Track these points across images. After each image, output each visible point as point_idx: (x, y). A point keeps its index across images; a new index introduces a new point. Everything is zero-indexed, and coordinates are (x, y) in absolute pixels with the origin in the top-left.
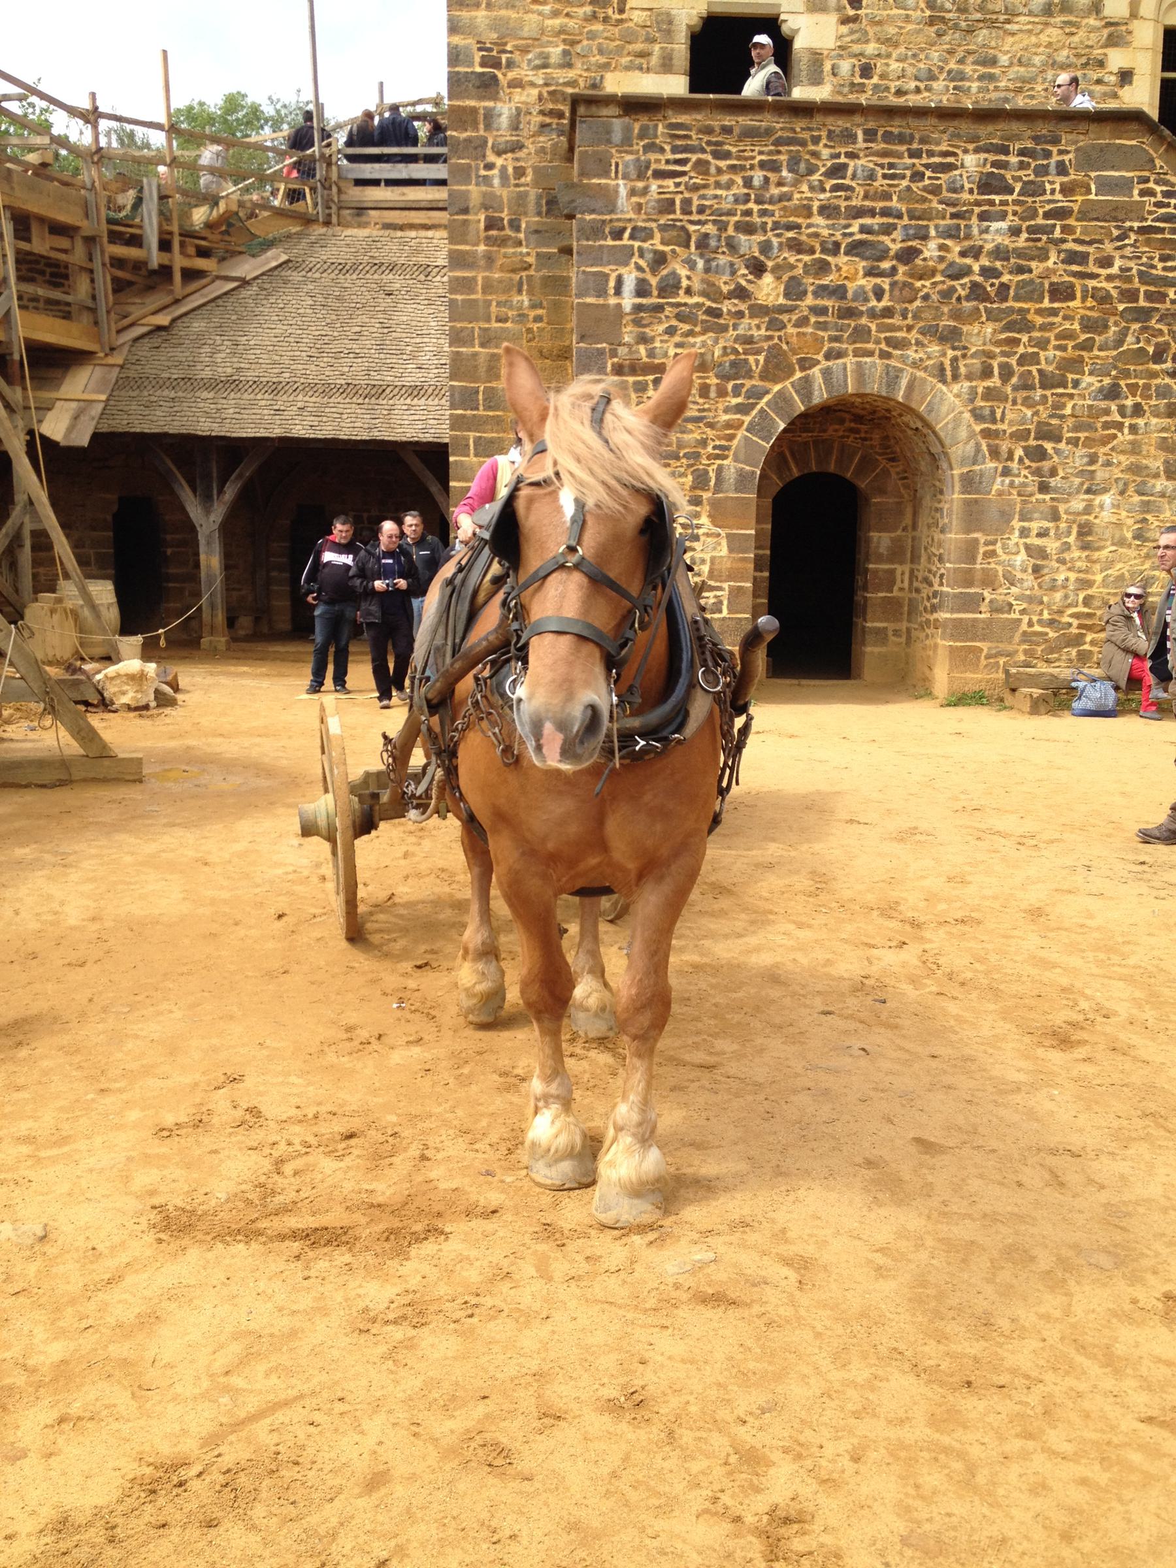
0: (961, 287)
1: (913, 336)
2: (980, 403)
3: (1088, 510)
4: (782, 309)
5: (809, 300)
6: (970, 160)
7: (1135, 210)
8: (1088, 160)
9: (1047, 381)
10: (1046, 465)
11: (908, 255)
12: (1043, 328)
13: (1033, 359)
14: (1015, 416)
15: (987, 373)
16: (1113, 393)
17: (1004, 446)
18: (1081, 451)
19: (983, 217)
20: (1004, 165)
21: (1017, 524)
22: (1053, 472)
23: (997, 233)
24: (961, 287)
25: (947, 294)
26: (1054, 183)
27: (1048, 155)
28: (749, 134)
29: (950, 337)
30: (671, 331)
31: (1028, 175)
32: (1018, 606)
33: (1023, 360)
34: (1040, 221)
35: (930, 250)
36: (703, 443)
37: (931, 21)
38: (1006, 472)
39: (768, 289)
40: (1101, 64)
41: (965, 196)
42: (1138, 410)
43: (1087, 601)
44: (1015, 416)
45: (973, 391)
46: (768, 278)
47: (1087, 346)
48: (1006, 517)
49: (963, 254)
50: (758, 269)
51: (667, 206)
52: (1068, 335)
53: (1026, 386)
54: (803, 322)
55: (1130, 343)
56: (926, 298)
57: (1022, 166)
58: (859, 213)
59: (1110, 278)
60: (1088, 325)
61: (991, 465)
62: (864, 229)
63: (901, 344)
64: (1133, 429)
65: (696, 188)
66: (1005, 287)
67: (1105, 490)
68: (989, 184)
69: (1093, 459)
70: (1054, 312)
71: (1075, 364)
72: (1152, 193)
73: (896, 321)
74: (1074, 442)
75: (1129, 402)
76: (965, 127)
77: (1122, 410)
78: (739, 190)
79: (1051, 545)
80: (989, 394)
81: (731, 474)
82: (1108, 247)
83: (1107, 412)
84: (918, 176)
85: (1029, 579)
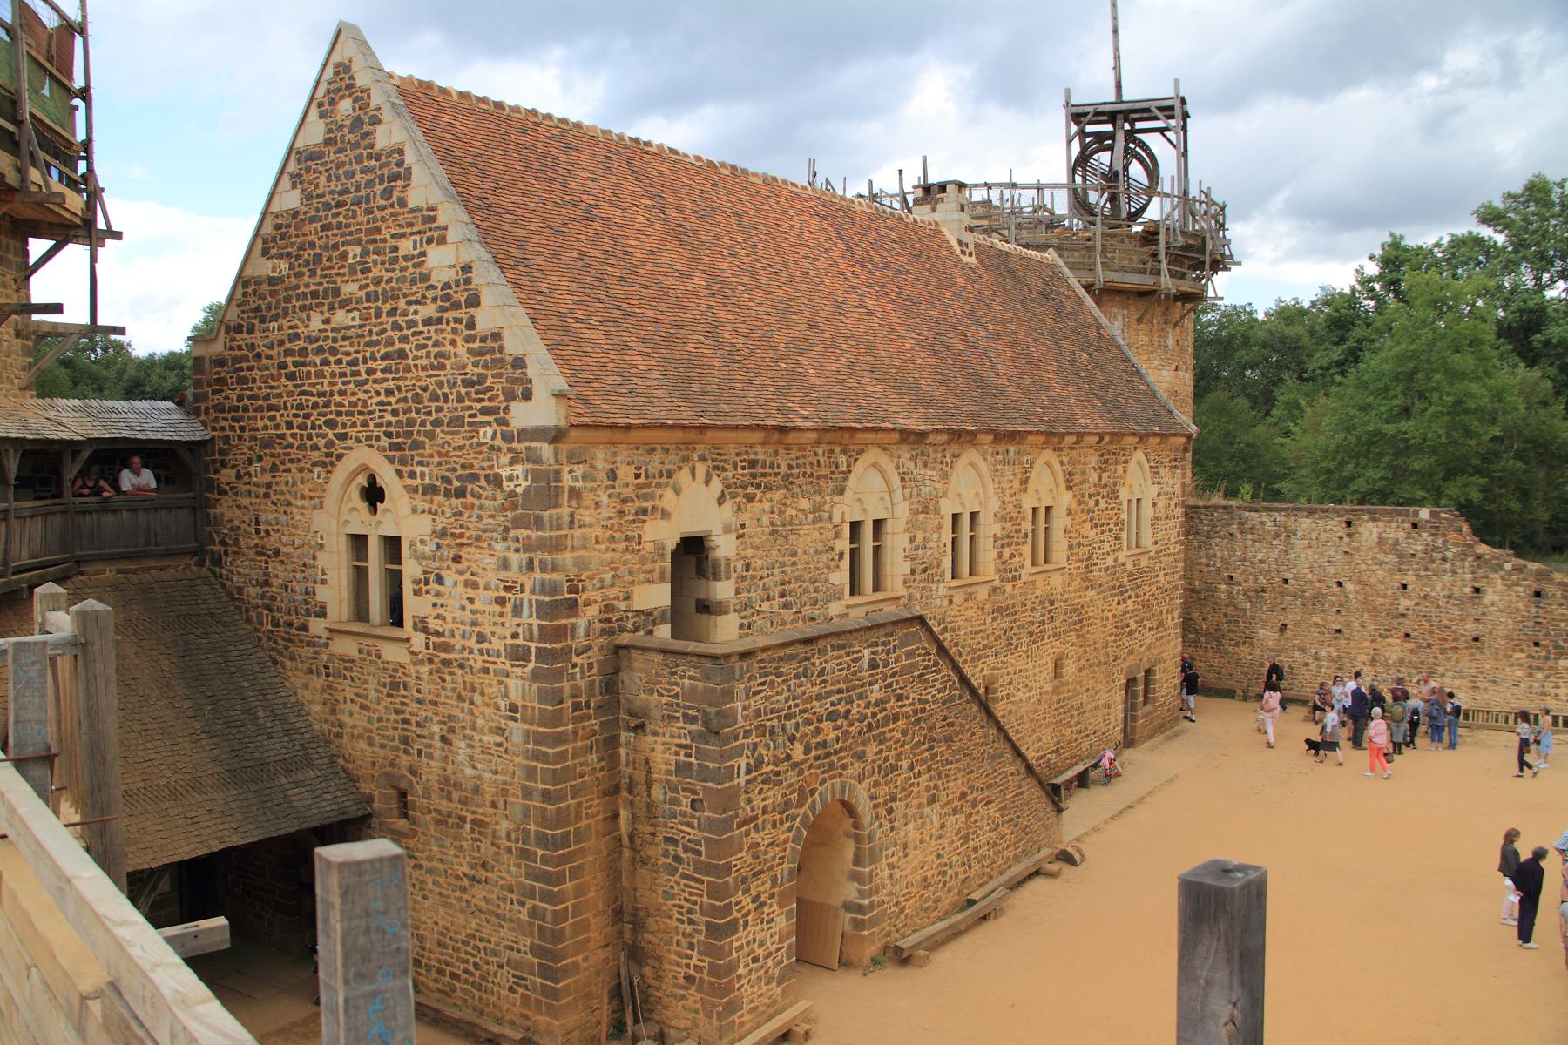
4: (803, 762)
5: (813, 753)
23: (876, 693)
28: (792, 657)
29: (860, 756)
30: (760, 792)
31: (884, 656)
36: (774, 858)
37: (772, 533)
39: (798, 752)
40: (832, 549)
46: (797, 744)
50: (792, 739)
51: (758, 714)
54: (810, 767)
58: (828, 694)
62: (833, 704)
65: (767, 698)
68: (873, 665)
71: (899, 757)
78: (786, 694)
81: (786, 873)
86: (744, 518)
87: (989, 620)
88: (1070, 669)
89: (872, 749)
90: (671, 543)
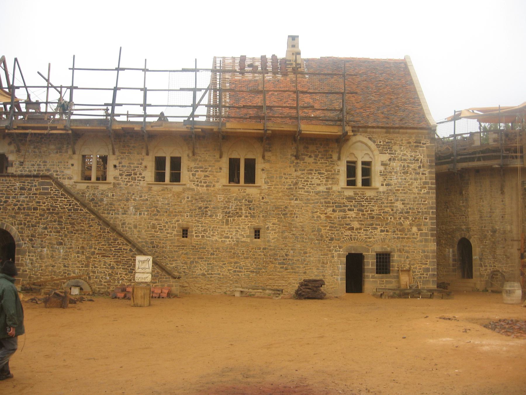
0: (16, 208)
1: (7, 217)
2: (20, 230)
3: (41, 251)
6: (18, 184)
7: (49, 193)
8: (41, 184)
9: (33, 226)
10: (33, 242)
11: (6, 202)
12: (32, 216)
13: (30, 222)
14: (27, 232)
15: (21, 224)
16: (46, 228)
17: (25, 238)
18: (40, 240)
19: (21, 195)
20: (25, 185)
21: (27, 254)
22: (34, 244)
23: (22, 198)
24: (16, 208)
25: (13, 209)
26: (34, 188)
27: (33, 183)
29: (14, 217)
31: (29, 187)
32: (28, 271)
33: (28, 222)
34: (31, 195)
35: (10, 201)
38: (25, 243)
41: (17, 191)
42: (51, 232)
43: (41, 270)
44: (27, 232)
45: (18, 228)
47: (41, 219)
48: (25, 253)
49: (17, 201)
52: (37, 217)
53: (29, 227)
55: (49, 219)
56: (9, 210)
57: (28, 185)
59: (45, 206)
60: (41, 215)
61: (22, 242)
63: (5, 218)
64: (50, 235)
66: (24, 208)
67: (45, 247)
68: (22, 189)
69: (42, 241)
70: (34, 213)
71: (39, 223)
72: (52, 190)
73: (4, 214)
74: (38, 238)
75: (49, 230)
76: (17, 178)
77: (48, 232)
79: (34, 259)
80: (22, 228)
82: (44, 200)
83: (45, 232)
84: (8, 187)
85: (30, 265)
88: (271, 236)
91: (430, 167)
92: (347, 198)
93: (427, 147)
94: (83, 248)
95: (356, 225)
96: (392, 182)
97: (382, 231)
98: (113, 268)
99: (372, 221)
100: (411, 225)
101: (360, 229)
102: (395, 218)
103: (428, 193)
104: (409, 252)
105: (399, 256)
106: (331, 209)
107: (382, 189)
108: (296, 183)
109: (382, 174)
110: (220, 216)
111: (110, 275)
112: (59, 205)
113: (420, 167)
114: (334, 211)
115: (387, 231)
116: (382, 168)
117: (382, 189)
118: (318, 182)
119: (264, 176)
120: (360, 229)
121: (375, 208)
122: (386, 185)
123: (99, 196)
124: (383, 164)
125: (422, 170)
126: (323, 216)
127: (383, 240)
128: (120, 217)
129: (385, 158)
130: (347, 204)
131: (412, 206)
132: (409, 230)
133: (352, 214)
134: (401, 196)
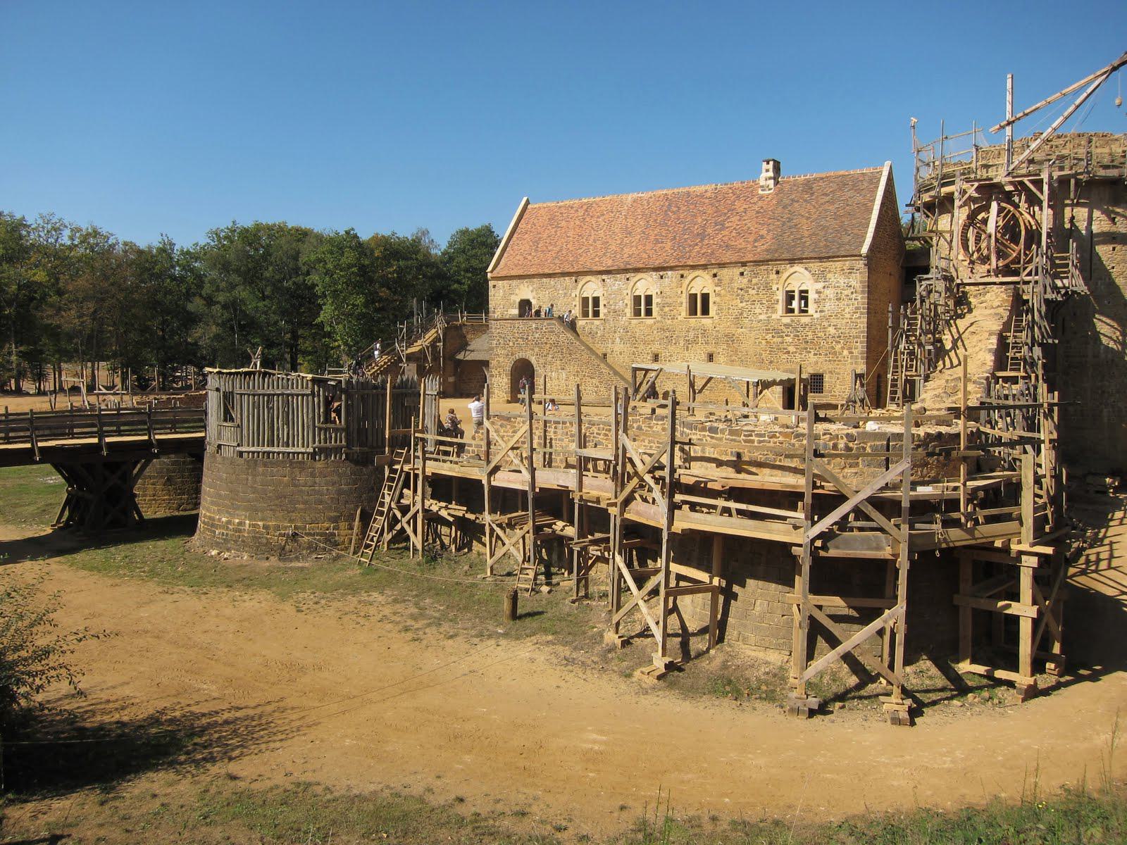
8: (548, 324)
23: (537, 336)
39: (511, 344)
44: (542, 361)
68: (537, 328)
86: (540, 295)
87: (655, 332)
89: (537, 350)
90: (518, 300)
91: (863, 292)
92: (785, 325)
93: (860, 273)
94: (577, 372)
95: (791, 349)
96: (824, 309)
97: (815, 354)
98: (597, 387)
99: (806, 345)
100: (843, 348)
101: (796, 352)
102: (827, 343)
103: (860, 318)
104: (839, 374)
105: (831, 378)
106: (770, 335)
107: (816, 315)
108: (741, 314)
109: (816, 302)
110: (682, 343)
111: (596, 392)
112: (561, 339)
113: (852, 293)
114: (773, 336)
115: (820, 354)
116: (816, 296)
117: (816, 316)
118: (760, 311)
119: (715, 308)
120: (796, 352)
121: (810, 333)
122: (821, 311)
123: (595, 330)
124: (818, 292)
125: (854, 295)
126: (764, 342)
127: (817, 363)
128: (609, 345)
129: (820, 286)
130: (785, 330)
131: (843, 331)
132: (840, 354)
133: (789, 339)
134: (834, 321)
